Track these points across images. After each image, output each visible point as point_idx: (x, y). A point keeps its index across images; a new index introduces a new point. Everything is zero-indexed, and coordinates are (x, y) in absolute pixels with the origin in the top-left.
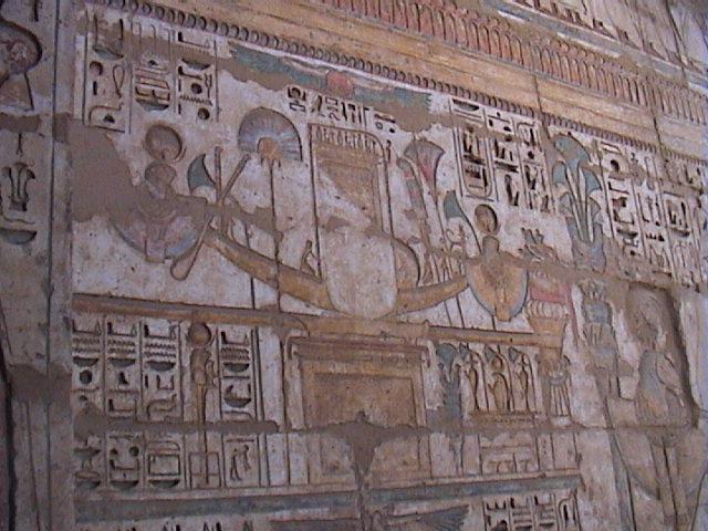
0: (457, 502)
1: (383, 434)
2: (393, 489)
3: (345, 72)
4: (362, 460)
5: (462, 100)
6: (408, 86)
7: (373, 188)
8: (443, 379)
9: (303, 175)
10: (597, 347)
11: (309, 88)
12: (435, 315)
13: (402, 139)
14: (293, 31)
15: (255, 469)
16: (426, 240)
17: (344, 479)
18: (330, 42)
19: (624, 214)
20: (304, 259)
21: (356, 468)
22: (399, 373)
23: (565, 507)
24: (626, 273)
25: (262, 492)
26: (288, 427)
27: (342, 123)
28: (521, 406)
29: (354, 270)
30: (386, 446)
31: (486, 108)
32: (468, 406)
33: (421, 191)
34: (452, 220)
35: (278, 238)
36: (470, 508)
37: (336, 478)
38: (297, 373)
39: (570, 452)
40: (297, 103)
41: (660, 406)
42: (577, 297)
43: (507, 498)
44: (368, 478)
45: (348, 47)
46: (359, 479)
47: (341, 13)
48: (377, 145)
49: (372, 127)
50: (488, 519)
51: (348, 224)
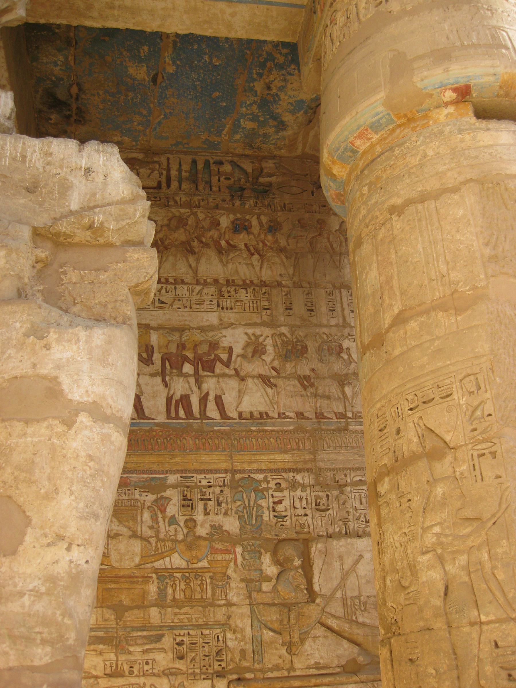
0: (160, 632)
2: (131, 627)
3: (127, 477)
5: (185, 475)
6: (157, 476)
7: (135, 520)
8: (159, 588)
16: (157, 536)
19: (280, 508)
24: (277, 535)
29: (123, 551)
30: (130, 612)
32: (170, 597)
36: (166, 635)
42: (239, 550)
43: (187, 631)
44: (120, 623)
46: (117, 624)
48: (139, 503)
49: (137, 496)
50: (175, 639)
51: (121, 535)
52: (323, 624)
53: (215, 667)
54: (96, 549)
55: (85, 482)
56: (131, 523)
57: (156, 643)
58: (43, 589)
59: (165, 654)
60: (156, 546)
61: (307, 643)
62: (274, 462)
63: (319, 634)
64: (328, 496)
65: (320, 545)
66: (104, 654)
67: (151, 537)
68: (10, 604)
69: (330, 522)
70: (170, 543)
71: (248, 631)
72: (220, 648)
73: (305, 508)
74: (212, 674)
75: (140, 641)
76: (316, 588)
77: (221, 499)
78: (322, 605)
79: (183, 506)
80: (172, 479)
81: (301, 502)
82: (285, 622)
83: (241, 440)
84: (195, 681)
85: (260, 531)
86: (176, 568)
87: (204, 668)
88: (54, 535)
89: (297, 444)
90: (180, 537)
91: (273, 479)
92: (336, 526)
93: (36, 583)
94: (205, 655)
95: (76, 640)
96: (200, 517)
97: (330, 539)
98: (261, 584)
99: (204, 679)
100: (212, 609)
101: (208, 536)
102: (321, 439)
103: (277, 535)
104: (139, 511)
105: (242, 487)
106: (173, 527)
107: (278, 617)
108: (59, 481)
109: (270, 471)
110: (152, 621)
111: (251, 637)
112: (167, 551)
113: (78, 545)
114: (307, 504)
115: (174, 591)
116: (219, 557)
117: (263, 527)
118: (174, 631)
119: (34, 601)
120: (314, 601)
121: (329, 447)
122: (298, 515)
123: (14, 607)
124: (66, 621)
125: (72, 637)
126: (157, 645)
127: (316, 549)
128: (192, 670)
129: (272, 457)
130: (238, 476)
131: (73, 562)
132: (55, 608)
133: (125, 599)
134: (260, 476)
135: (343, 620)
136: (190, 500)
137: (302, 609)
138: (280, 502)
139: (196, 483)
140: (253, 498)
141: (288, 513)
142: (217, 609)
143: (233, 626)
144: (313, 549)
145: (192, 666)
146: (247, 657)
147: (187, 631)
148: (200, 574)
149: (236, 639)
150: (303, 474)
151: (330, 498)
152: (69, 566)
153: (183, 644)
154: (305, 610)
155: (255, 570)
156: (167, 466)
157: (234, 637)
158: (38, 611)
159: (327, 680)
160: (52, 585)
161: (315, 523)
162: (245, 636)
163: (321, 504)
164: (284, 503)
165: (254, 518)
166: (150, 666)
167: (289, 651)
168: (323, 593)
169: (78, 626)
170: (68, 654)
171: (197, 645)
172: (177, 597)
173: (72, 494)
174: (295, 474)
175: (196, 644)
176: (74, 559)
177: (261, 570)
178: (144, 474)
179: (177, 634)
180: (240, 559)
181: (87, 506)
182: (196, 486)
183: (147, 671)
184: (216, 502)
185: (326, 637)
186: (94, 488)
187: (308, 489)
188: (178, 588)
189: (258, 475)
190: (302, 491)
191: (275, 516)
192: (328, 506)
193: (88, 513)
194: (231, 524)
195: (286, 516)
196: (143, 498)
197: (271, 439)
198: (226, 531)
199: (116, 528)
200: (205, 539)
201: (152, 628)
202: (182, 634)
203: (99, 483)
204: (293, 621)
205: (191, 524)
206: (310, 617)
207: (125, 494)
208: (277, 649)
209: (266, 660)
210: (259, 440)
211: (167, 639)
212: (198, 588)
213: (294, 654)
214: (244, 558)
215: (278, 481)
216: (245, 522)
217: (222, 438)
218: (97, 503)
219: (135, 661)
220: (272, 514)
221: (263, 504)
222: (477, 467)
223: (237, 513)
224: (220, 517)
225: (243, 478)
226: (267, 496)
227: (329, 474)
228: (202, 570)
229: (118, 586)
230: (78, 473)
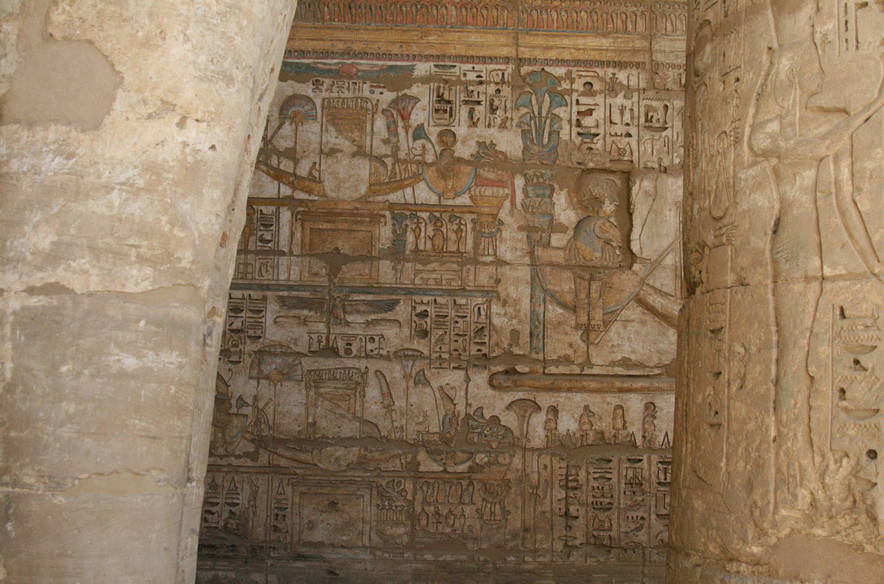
0: (393, 297)
1: (347, 259)
4: (334, 271)
5: (442, 63)
6: (399, 63)
7: (362, 130)
8: (394, 232)
9: (316, 127)
10: (533, 213)
11: (325, 77)
12: (394, 197)
13: (389, 96)
14: (320, 45)
15: (271, 272)
16: (394, 155)
17: (321, 280)
18: (345, 46)
19: (588, 121)
20: (310, 173)
21: (329, 275)
22: (363, 228)
23: (479, 308)
24: (579, 164)
25: (273, 282)
26: (291, 253)
27: (347, 94)
28: (453, 248)
29: (341, 175)
30: (350, 265)
31: (462, 65)
32: (410, 247)
33: (397, 127)
34: (418, 141)
35: (296, 162)
36: (402, 302)
37: (316, 279)
38: (299, 229)
39: (491, 277)
40: (317, 88)
41: (592, 252)
42: (519, 182)
43: (433, 298)
44: (336, 280)
45: (357, 47)
46: (330, 281)
47: (356, 26)
48: (369, 104)
49: (366, 93)
50: (414, 308)
51: (341, 151)
52: (641, 302)
53: (472, 353)
54: (230, 129)
55: (209, 23)
56: (356, 135)
57: (386, 312)
58: (141, 183)
59: (398, 329)
60: (394, 169)
61: (613, 329)
62: (585, 49)
63: (633, 317)
64: (666, 107)
65: (646, 183)
66: (310, 324)
67: (386, 156)
68: (91, 203)
69: (666, 149)
70: (414, 168)
71: (525, 305)
72: (480, 326)
73: (628, 124)
74: (468, 362)
75: (363, 308)
76: (635, 247)
77: (497, 102)
78: (642, 274)
79: (437, 111)
80: (422, 68)
81: (622, 114)
82: (583, 296)
83: (534, 13)
84: (440, 370)
85: (553, 157)
86: (422, 204)
87: (455, 353)
88: (159, 103)
89: (625, 23)
90: (430, 158)
91: (580, 76)
92: (675, 155)
93: (130, 173)
94: (457, 334)
95: (193, 262)
96: (461, 129)
97: (664, 176)
98: (550, 236)
99: (454, 368)
100: (472, 268)
101: (473, 159)
102: (663, 15)
103: (579, 164)
104: (369, 117)
105: (531, 86)
106: (419, 143)
107: (573, 287)
108: (166, 20)
109: (577, 62)
110: (382, 280)
111: (528, 314)
112: (410, 178)
113: (197, 120)
114: (632, 118)
115: (417, 238)
116: (489, 192)
117: (559, 150)
118: (414, 297)
119: (127, 200)
120: (630, 268)
121: (674, 30)
122: (616, 135)
123: (97, 206)
124: (176, 231)
125: (186, 258)
126: (388, 316)
127: (640, 188)
128: (438, 355)
129: (580, 42)
130: (525, 69)
131: (188, 145)
132: (159, 212)
133: (345, 246)
134: (560, 71)
135: (672, 298)
136: (449, 102)
137: (610, 277)
138: (590, 112)
139: (459, 76)
140: (546, 104)
141: (601, 131)
142: (480, 268)
143: (502, 295)
144: (635, 189)
145: (437, 349)
146: (521, 343)
147: (433, 298)
148: (457, 215)
149: (505, 314)
150: (628, 71)
151: (670, 111)
152: (183, 151)
153: (427, 316)
154: (615, 279)
155: (544, 214)
156: (414, 48)
157: (503, 312)
158: (132, 214)
159: (639, 384)
160: (154, 178)
161: (642, 148)
162: (519, 311)
163: (654, 120)
164: (594, 113)
165: (546, 135)
166: (376, 345)
167: (585, 339)
168: (645, 255)
169: (197, 242)
170: (179, 281)
171: (448, 319)
172: (421, 247)
173: (187, 39)
174: (616, 71)
175: (446, 316)
176: (191, 141)
177: (552, 215)
178: (379, 59)
179: (418, 301)
180: (519, 196)
181: (212, 61)
182: (459, 82)
183: (372, 351)
184: (488, 108)
185: (643, 322)
186: (224, 33)
187: (636, 95)
188: (423, 234)
189: (557, 69)
190: (625, 97)
191: (579, 134)
192: (665, 122)
193: (213, 71)
194: (510, 143)
195: (597, 135)
196: (376, 96)
197: (583, 13)
198: (501, 152)
199: (333, 140)
200: (468, 163)
201: (382, 290)
202: (425, 301)
203: (232, 29)
204: (594, 295)
205: (447, 138)
206: (622, 291)
207: (348, 89)
208: (566, 334)
209: (548, 348)
210: (563, 13)
211: (403, 308)
212: (453, 237)
213: (593, 343)
214: (526, 195)
215: (589, 80)
216: (532, 141)
217: (504, 8)
218: (230, 58)
219: (355, 336)
220: (575, 130)
221: (561, 115)
222: (851, 25)
223: (521, 127)
224: (492, 130)
225: (533, 72)
226: (569, 102)
227: (670, 73)
228: (460, 209)
229: (334, 227)
230: (198, 9)
